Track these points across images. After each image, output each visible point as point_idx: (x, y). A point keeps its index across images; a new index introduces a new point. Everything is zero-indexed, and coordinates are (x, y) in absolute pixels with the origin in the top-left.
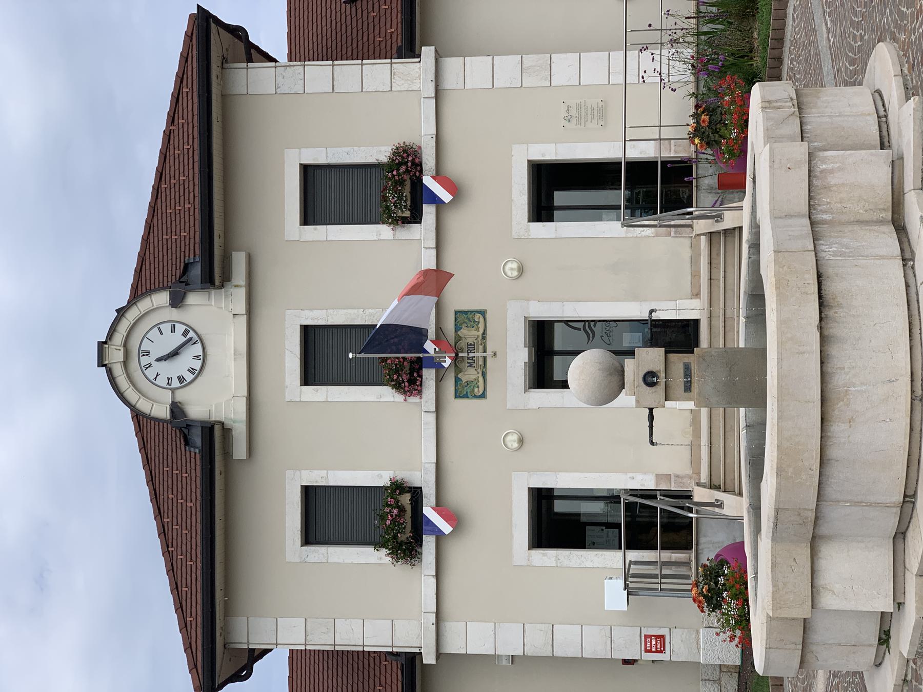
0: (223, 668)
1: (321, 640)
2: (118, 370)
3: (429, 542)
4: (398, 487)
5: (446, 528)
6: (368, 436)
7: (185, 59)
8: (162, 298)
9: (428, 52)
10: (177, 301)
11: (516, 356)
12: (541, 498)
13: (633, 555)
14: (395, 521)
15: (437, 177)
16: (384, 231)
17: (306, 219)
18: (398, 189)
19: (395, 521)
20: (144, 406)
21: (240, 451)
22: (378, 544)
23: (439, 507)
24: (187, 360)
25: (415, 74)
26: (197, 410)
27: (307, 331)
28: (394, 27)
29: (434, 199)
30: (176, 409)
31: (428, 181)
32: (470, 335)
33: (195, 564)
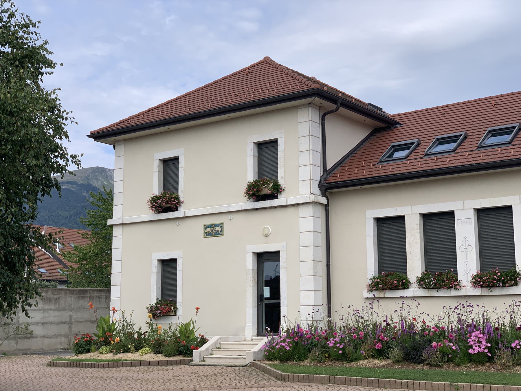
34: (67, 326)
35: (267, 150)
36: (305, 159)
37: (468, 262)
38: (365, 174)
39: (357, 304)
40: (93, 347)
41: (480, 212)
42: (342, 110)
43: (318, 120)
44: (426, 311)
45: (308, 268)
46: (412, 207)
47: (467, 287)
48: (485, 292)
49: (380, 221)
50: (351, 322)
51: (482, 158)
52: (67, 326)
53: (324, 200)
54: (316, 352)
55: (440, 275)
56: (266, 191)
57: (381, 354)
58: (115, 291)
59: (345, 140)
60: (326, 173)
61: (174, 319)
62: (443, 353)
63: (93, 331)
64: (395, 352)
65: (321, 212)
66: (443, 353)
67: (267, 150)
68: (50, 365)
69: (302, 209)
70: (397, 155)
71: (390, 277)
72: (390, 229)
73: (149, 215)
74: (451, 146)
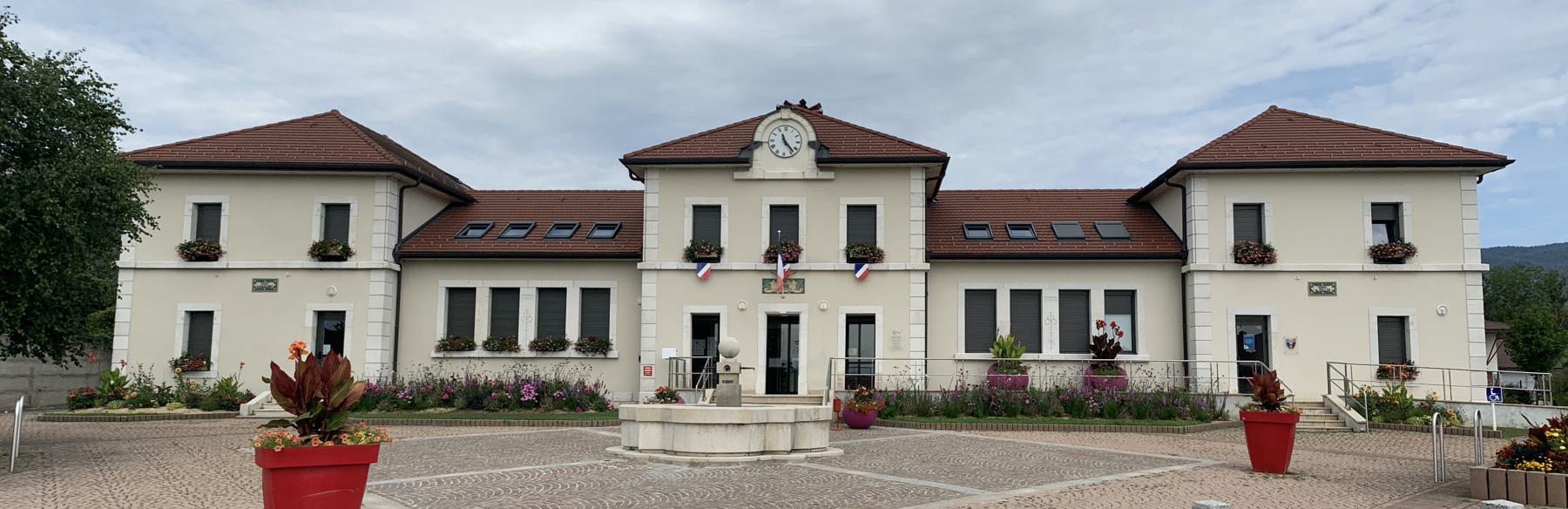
0: (635, 168)
1: (648, 214)
2: (778, 116)
3: (694, 266)
4: (720, 251)
5: (701, 274)
6: (744, 236)
7: (927, 149)
8: (813, 138)
9: (927, 266)
10: (811, 144)
11: (783, 307)
12: (715, 318)
13: (689, 362)
14: (704, 249)
15: (868, 271)
16: (843, 245)
17: (849, 207)
18: (863, 251)
19: (704, 249)
20: (761, 128)
21: (738, 175)
22: (693, 242)
23: (711, 271)
24: (783, 149)
25: (918, 260)
26: (758, 153)
27: (796, 207)
28: (943, 250)
29: (858, 269)
30: (759, 144)
31: (866, 266)
32: (793, 286)
33: (684, 155)
34: (26, 381)
35: (336, 215)
36: (380, 227)
37: (527, 331)
38: (440, 248)
39: (422, 360)
40: (97, 402)
41: (541, 291)
42: (422, 185)
43: (397, 193)
44: (490, 369)
45: (376, 329)
46: (483, 282)
47: (525, 351)
48: (540, 355)
49: (452, 291)
50: (420, 377)
51: (546, 248)
52: (26, 381)
53: (397, 268)
54: (385, 403)
55: (503, 340)
56: (334, 252)
57: (447, 403)
58: (119, 343)
59: (421, 212)
60: (401, 241)
61: (205, 374)
62: (500, 401)
63: (93, 384)
64: (460, 401)
65: (393, 278)
66: (500, 401)
67: (336, 215)
68: (39, 419)
69: (374, 276)
70: (471, 233)
71: (457, 339)
72: (461, 300)
73: (178, 262)
74: (523, 232)
